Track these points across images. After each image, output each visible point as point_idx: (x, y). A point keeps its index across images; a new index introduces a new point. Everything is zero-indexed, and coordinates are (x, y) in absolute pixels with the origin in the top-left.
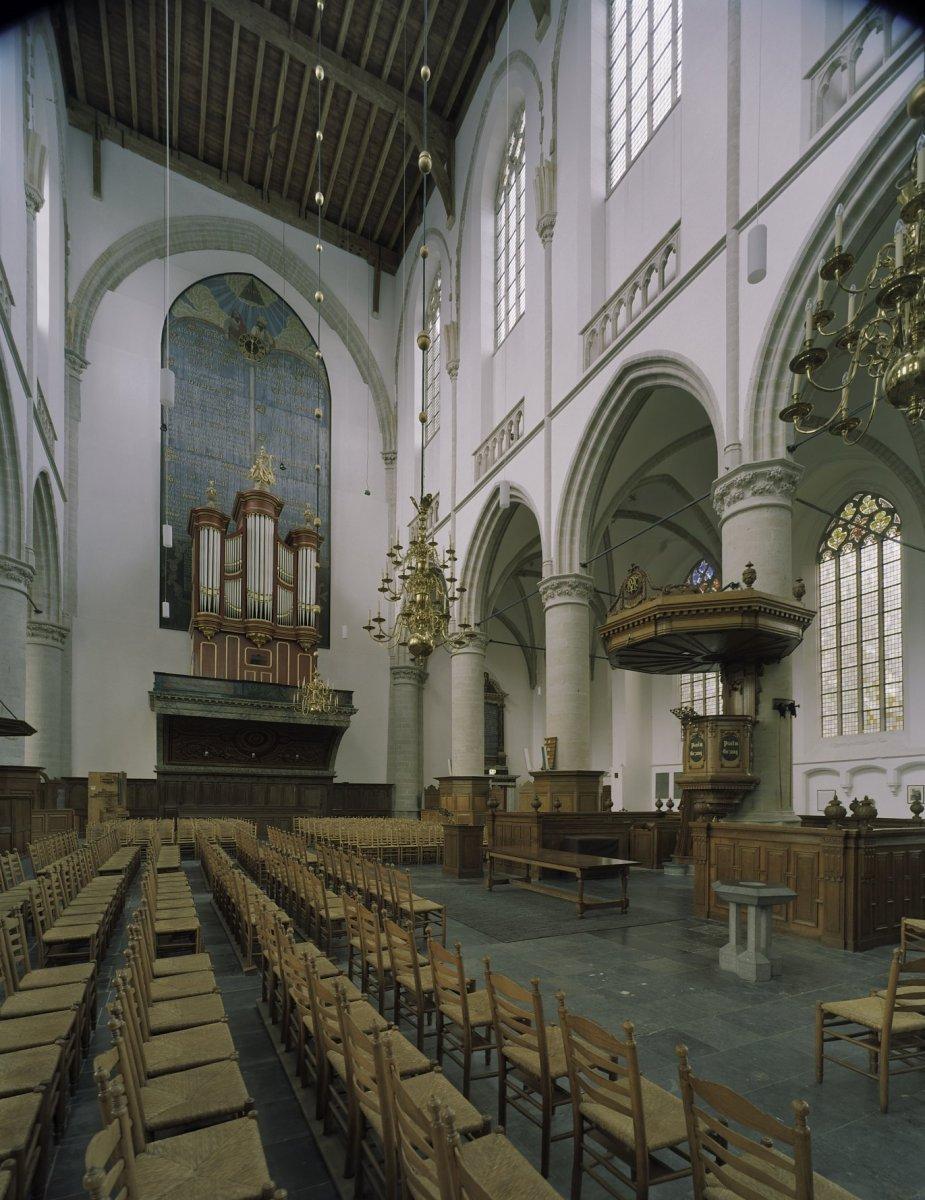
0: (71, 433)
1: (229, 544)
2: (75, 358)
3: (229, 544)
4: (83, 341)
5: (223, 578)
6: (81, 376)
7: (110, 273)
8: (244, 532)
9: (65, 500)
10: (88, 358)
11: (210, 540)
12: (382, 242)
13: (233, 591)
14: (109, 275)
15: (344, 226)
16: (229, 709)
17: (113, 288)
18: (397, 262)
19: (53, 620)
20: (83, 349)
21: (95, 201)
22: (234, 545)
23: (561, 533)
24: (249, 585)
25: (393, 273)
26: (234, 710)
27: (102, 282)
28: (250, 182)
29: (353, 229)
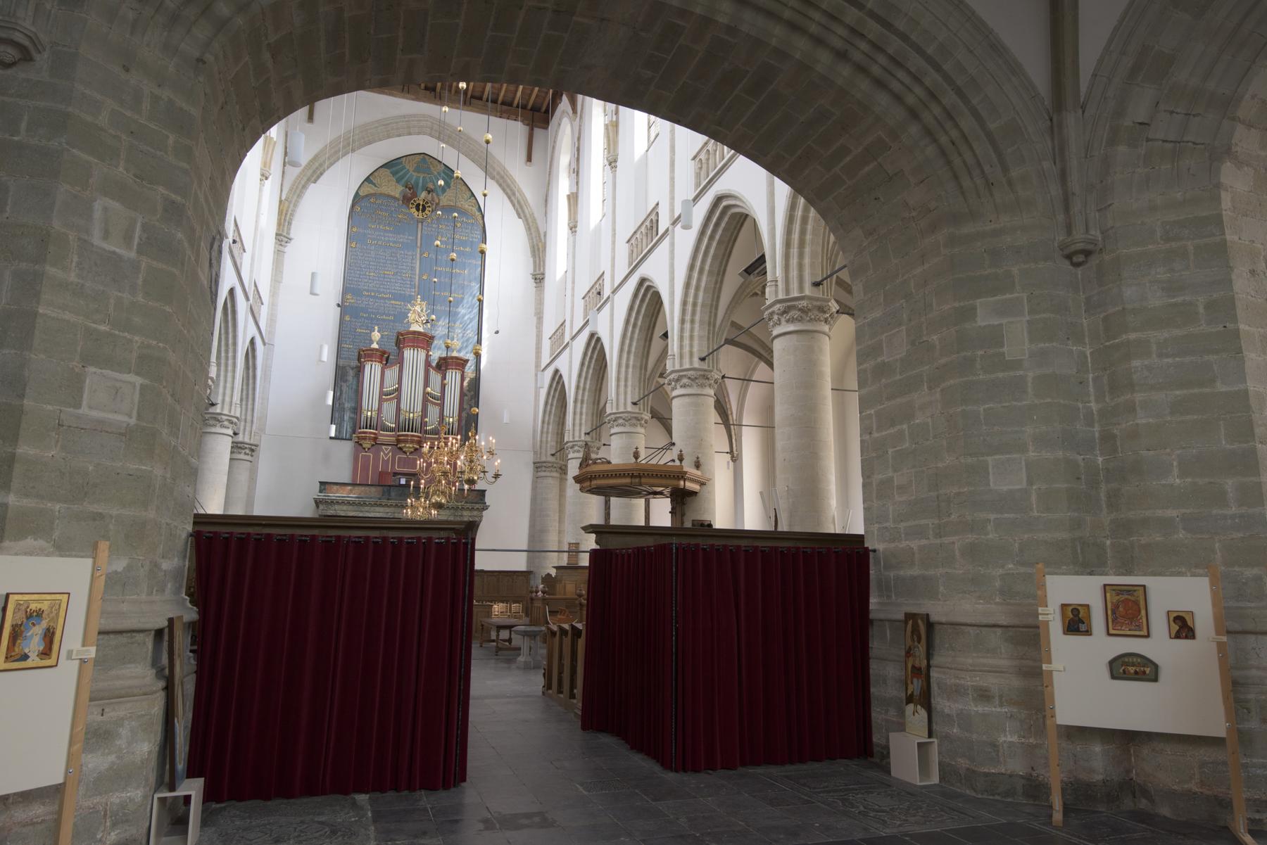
0: (274, 293)
1: (388, 372)
2: (282, 237)
3: (388, 372)
4: (290, 224)
5: (381, 401)
6: (286, 250)
7: (314, 172)
8: (400, 362)
9: (264, 344)
10: (292, 236)
11: (372, 370)
12: (535, 109)
13: (389, 410)
14: (315, 172)
15: (503, 103)
16: (377, 509)
17: (315, 182)
18: (548, 123)
19: (247, 440)
20: (289, 229)
21: (309, 125)
22: (391, 373)
23: (621, 350)
24: (402, 406)
25: (546, 128)
26: (381, 509)
27: (309, 180)
28: (426, 88)
29: (511, 104)
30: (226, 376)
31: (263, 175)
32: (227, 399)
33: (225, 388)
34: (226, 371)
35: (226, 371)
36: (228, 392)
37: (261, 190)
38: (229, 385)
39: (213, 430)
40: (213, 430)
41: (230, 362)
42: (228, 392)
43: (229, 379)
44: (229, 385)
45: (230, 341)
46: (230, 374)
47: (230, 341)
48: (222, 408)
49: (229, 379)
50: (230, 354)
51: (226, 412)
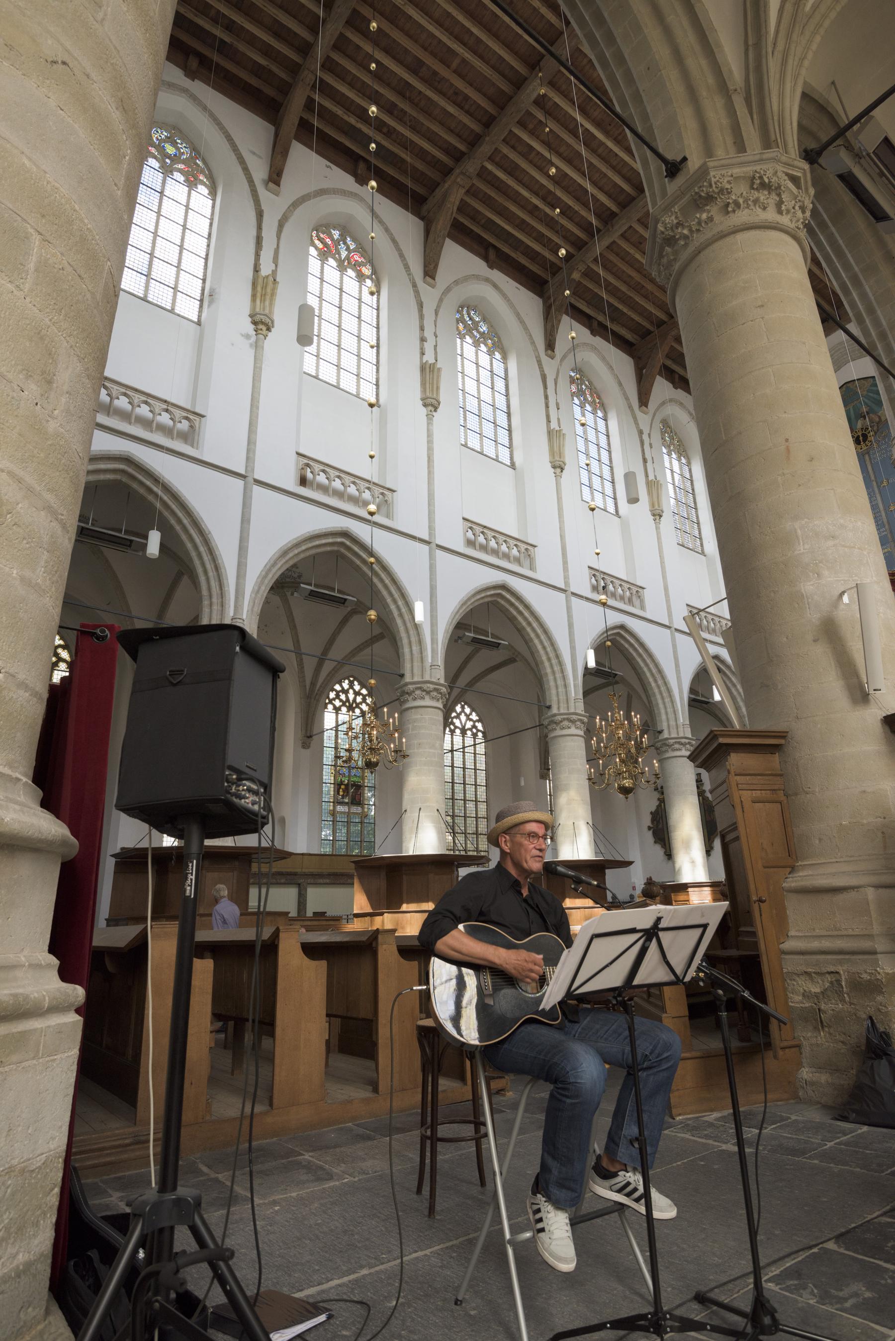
30: (664, 703)
31: (654, 515)
32: (672, 723)
33: (667, 713)
34: (663, 698)
35: (663, 698)
36: (671, 716)
37: (657, 528)
38: (670, 710)
39: (667, 755)
40: (667, 755)
41: (663, 688)
42: (671, 716)
43: (669, 705)
44: (670, 710)
45: (654, 671)
46: (667, 700)
47: (654, 671)
48: (670, 733)
49: (669, 705)
50: (660, 682)
51: (674, 735)
